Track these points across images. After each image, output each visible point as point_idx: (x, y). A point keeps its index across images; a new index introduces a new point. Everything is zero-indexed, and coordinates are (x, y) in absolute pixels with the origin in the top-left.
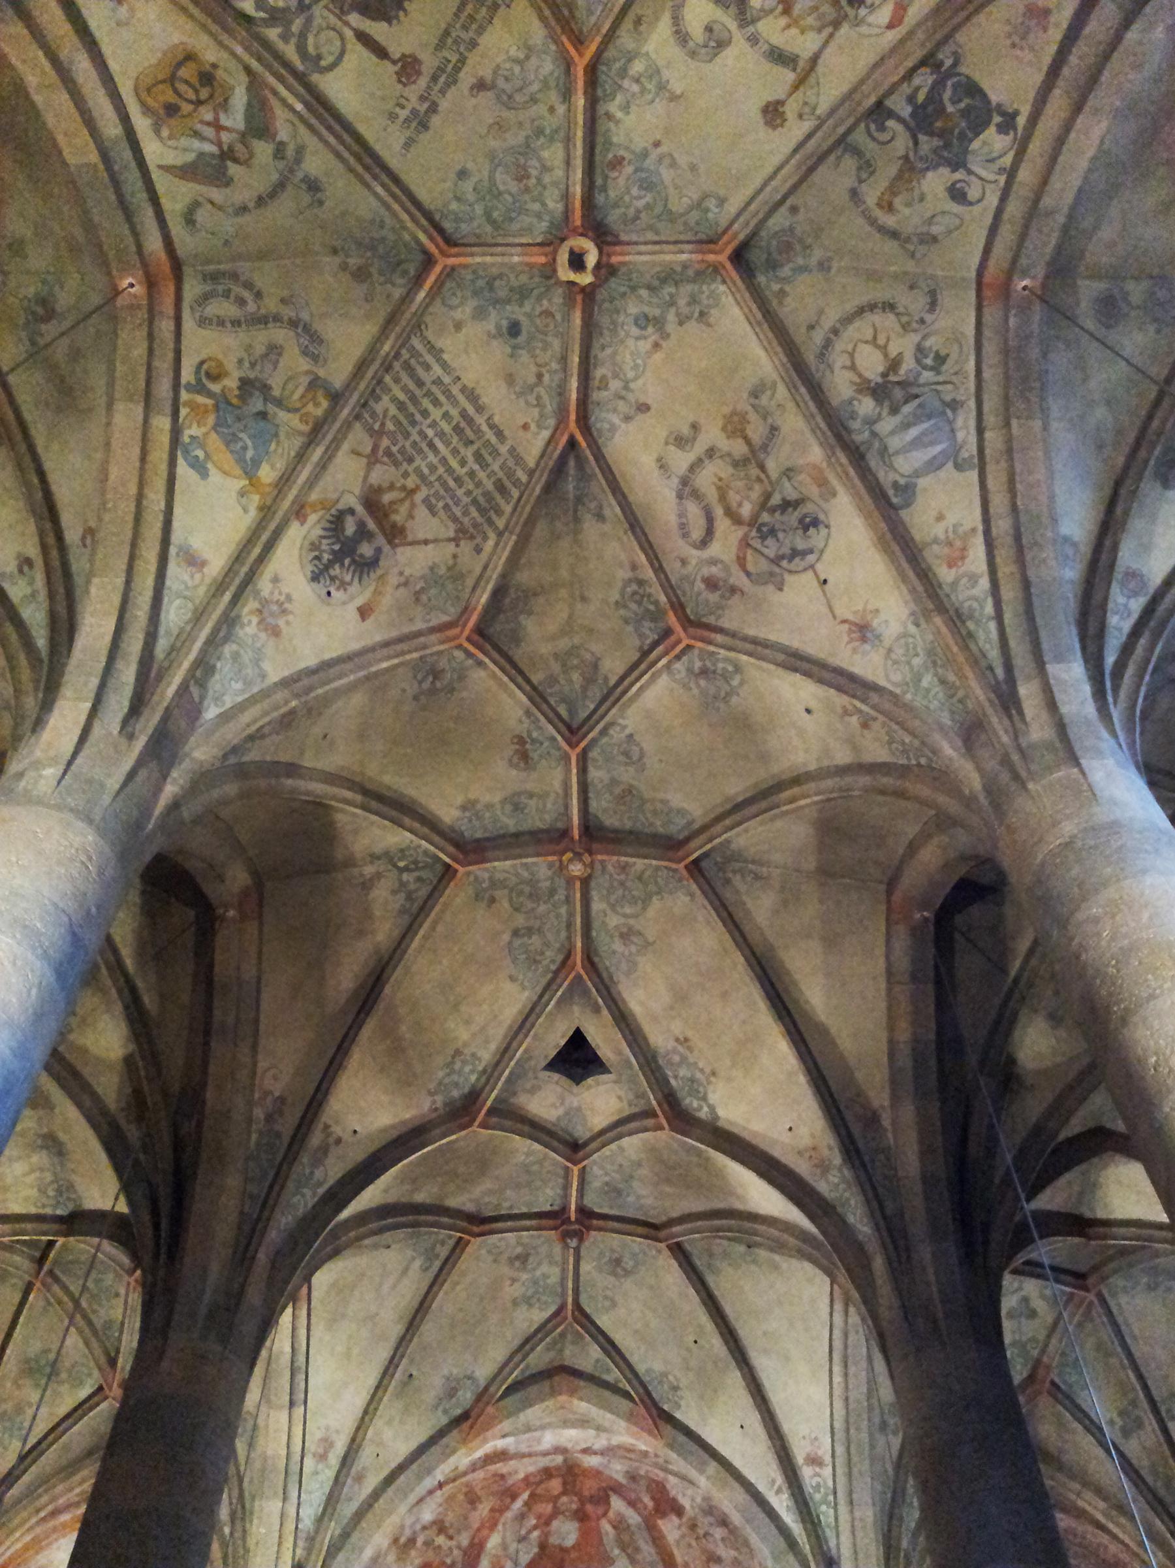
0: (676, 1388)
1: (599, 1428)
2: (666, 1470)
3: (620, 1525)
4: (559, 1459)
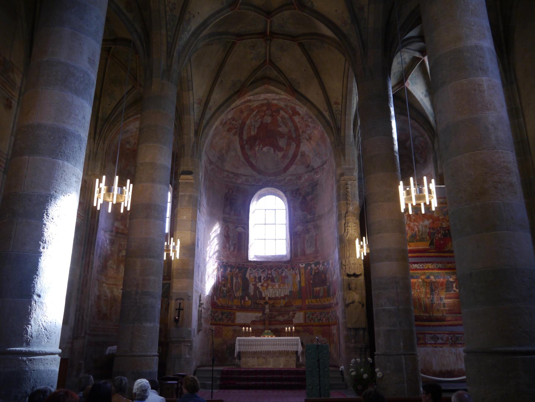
0: (299, 83)
1: (277, 93)
2: (295, 104)
3: (282, 118)
4: (266, 101)
